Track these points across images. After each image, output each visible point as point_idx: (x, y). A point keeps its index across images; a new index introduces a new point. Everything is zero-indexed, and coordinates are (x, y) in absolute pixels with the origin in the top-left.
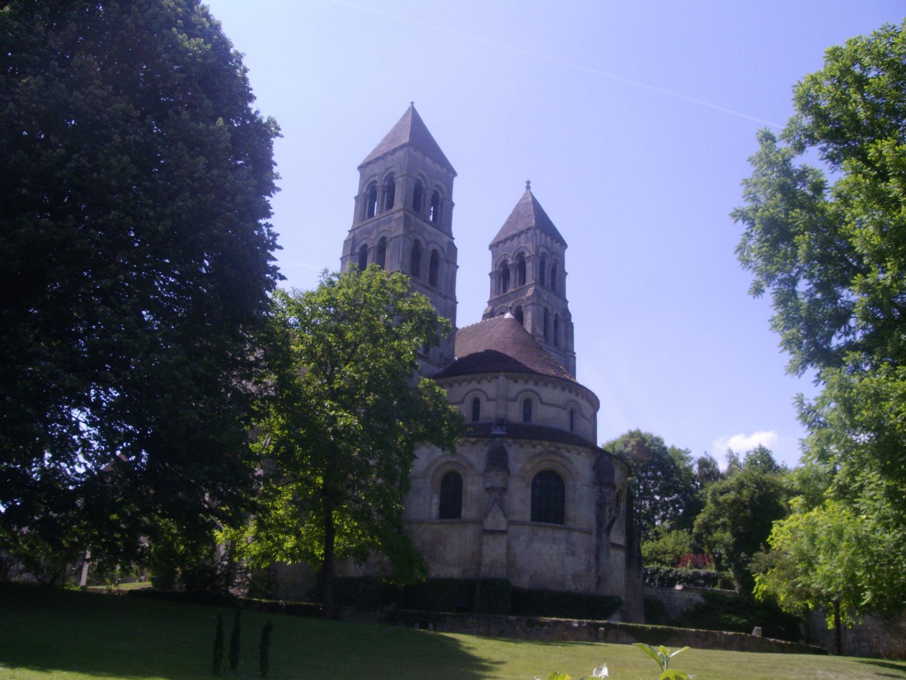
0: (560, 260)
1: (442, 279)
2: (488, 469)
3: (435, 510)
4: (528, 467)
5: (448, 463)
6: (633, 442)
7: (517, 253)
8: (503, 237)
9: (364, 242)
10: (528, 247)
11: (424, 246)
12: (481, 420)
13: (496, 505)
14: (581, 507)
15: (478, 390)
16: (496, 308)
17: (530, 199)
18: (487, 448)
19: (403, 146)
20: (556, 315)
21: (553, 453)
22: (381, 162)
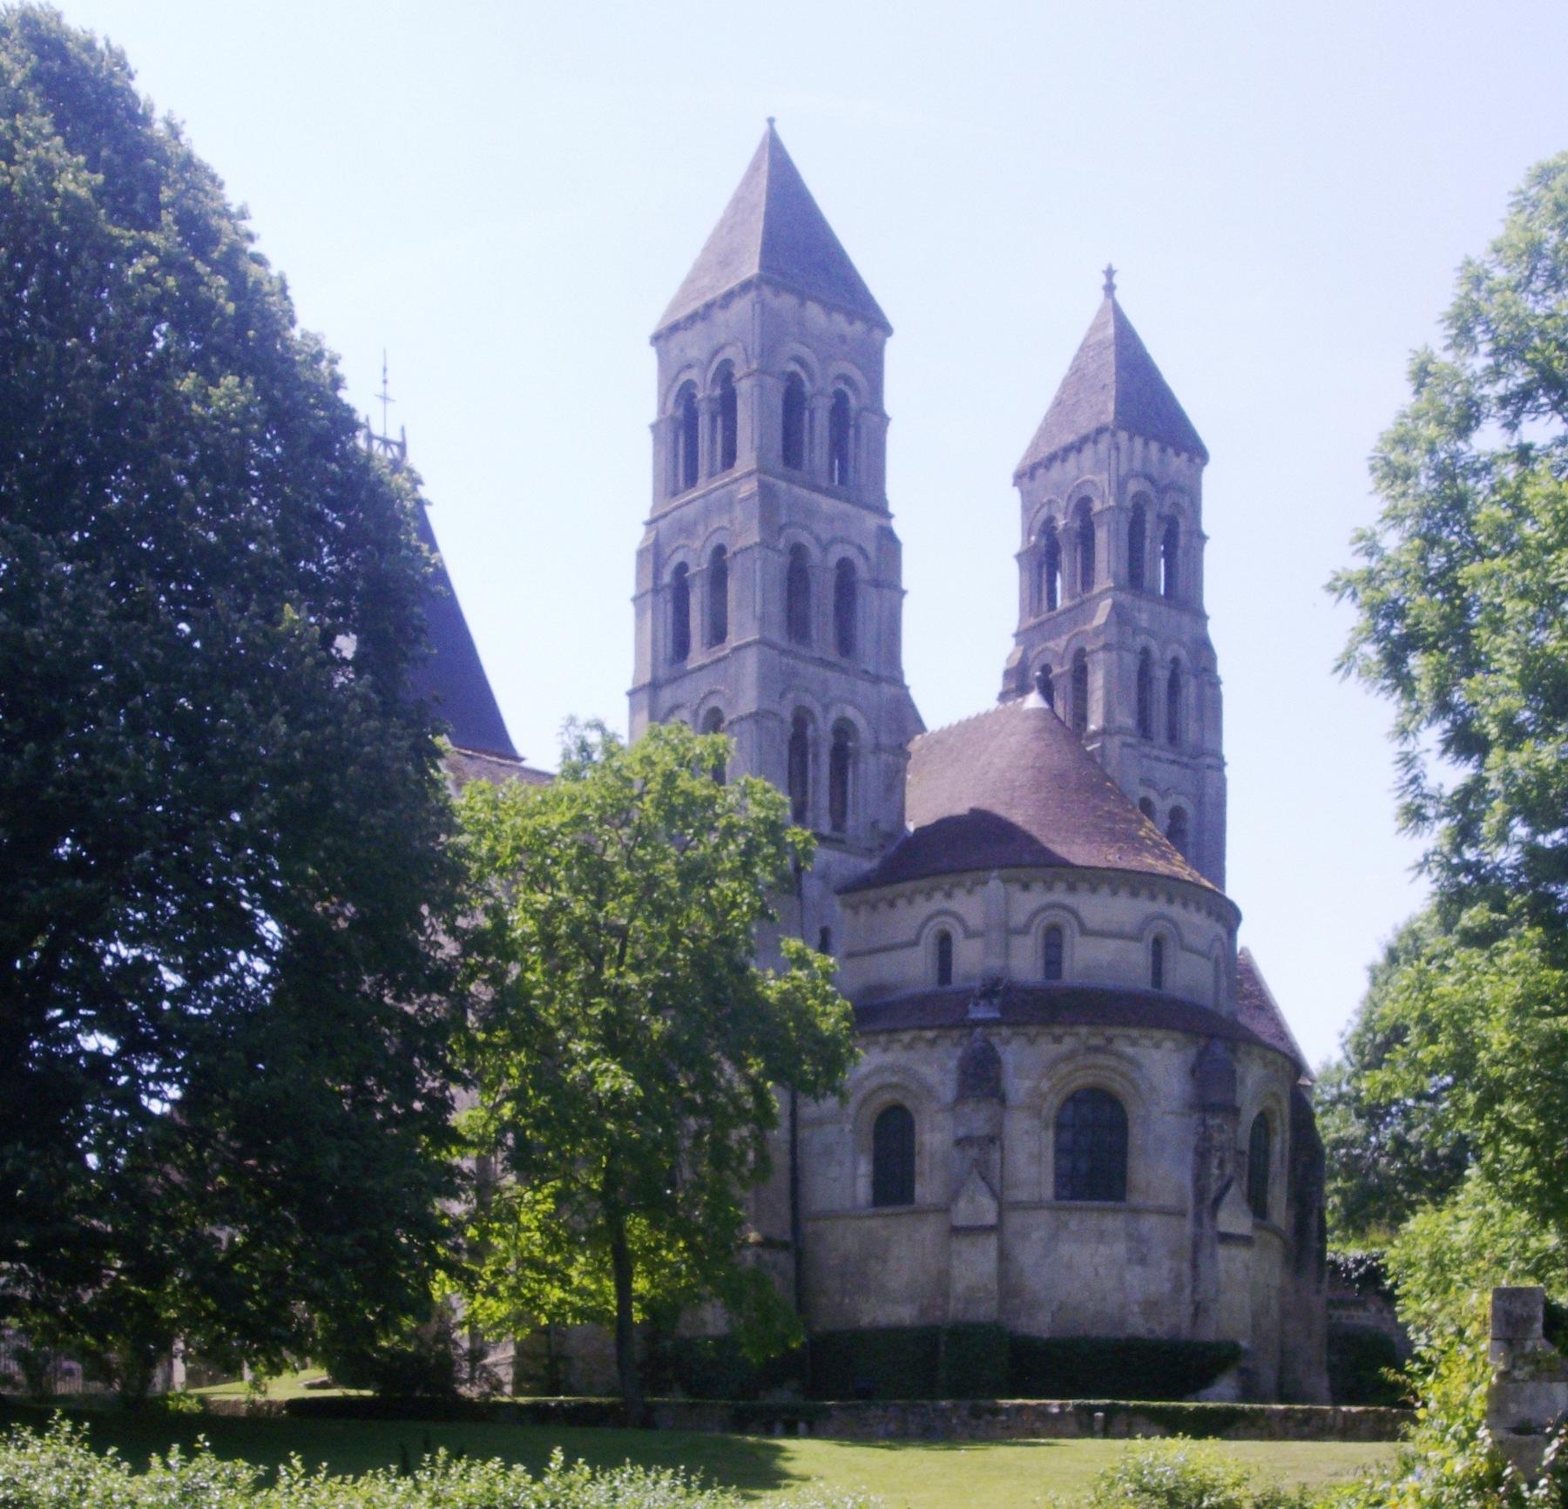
2: (961, 1098)
4: (1045, 1085)
5: (881, 1088)
10: (1096, 477)
12: (957, 981)
15: (945, 912)
16: (1032, 654)
18: (959, 1052)
21: (1097, 1050)
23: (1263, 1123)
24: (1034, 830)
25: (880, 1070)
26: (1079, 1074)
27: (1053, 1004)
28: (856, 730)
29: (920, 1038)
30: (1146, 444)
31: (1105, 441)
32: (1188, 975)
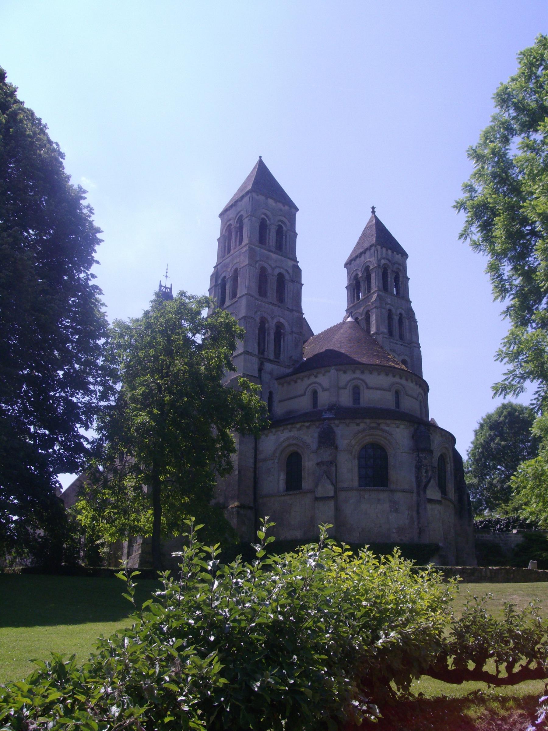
0: (401, 268)
1: (288, 297)
3: (282, 485)
4: (353, 442)
6: (505, 413)
7: (364, 267)
8: (354, 255)
9: (224, 275)
10: (371, 260)
11: (269, 270)
12: (319, 408)
13: (325, 476)
14: (402, 472)
17: (374, 221)
18: (319, 430)
19: (247, 193)
20: (401, 314)
21: (373, 428)
22: (234, 208)
23: (442, 458)
24: (348, 354)
25: (288, 438)
26: (368, 437)
27: (355, 413)
28: (284, 326)
29: (303, 426)
30: (387, 250)
31: (373, 248)
32: (408, 404)
